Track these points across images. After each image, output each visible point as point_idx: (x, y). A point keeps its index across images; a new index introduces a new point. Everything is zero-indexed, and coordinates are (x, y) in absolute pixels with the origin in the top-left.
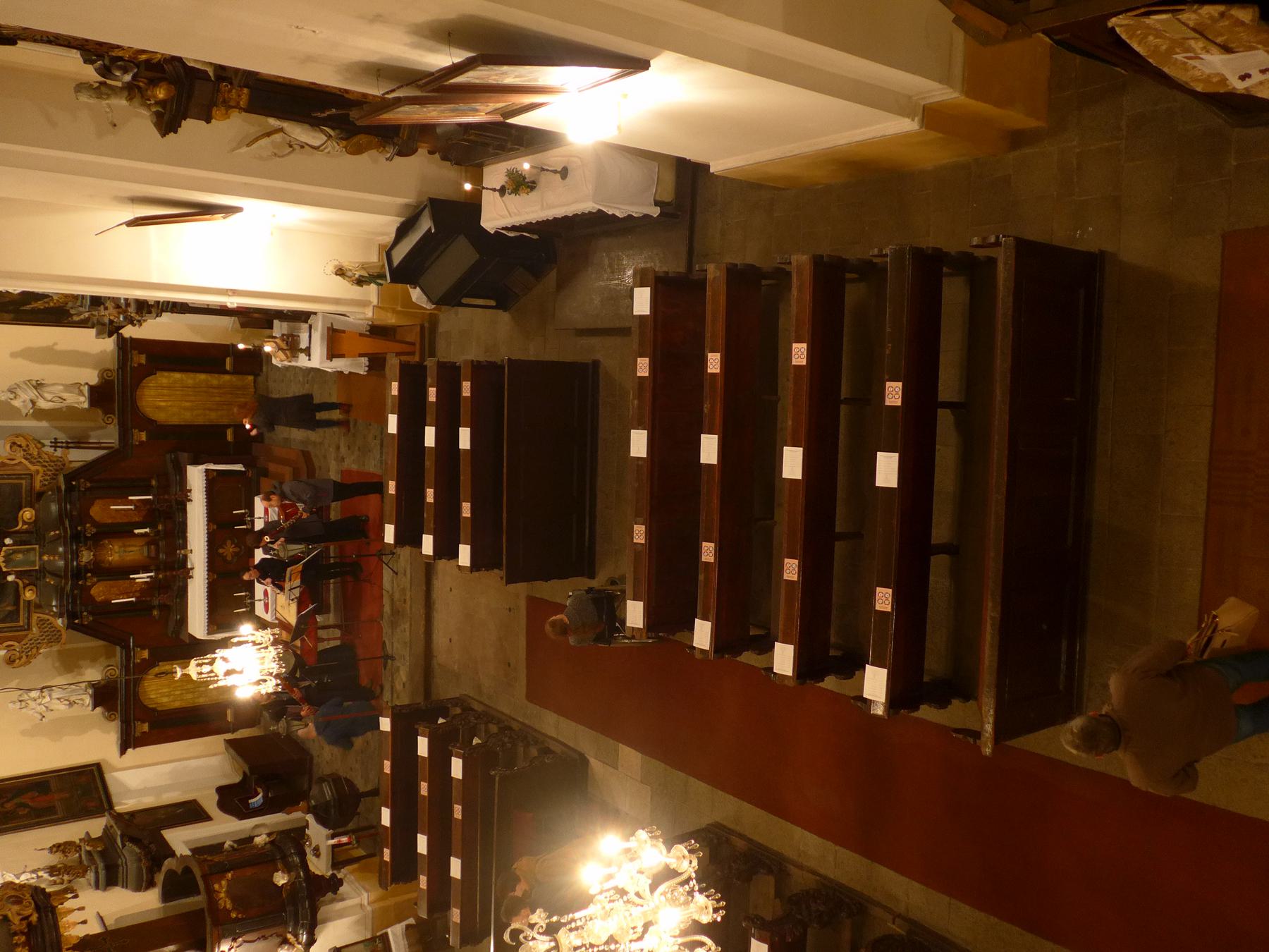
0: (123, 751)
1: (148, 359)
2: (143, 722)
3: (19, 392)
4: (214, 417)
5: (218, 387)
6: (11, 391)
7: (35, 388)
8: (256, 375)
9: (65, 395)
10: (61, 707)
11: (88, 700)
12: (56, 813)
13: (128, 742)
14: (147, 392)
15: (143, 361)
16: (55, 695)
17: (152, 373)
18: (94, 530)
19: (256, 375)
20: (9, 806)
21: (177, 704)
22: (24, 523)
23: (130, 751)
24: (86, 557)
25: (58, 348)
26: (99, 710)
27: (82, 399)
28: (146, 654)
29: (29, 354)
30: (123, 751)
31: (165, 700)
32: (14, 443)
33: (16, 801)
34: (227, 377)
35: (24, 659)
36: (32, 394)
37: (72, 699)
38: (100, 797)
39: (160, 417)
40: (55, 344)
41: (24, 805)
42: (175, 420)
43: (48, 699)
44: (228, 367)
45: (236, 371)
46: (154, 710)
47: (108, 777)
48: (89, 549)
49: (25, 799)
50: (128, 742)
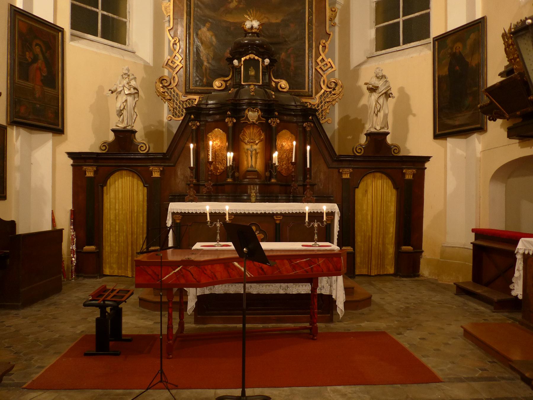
0: (71, 155)
1: (409, 180)
2: (95, 172)
3: (383, 80)
4: (358, 239)
5: (384, 244)
6: (383, 77)
7: (386, 93)
8: (395, 275)
9: (381, 114)
10: (119, 104)
11: (121, 126)
12: (20, 78)
13: (79, 159)
14: (379, 183)
15: (407, 177)
16: (130, 99)
17: (396, 186)
18: (274, 125)
19: (395, 275)
20: (37, 49)
21: (107, 205)
22: (277, 83)
23: (71, 162)
24: (253, 115)
25: (411, 118)
26: (111, 137)
27: (378, 128)
28: (156, 174)
29: (404, 97)
30: (71, 155)
31: (112, 194)
32: (336, 84)
33: (41, 56)
34: (391, 250)
35: (162, 90)
36: (382, 89)
37: (125, 112)
38: (29, 119)
39: (359, 193)
40: (414, 115)
41: (35, 59)
42: (357, 207)
43: (127, 92)
44: (405, 248)
45: (399, 254)
46: (105, 183)
47: (50, 135)
48: (259, 119)
49: (40, 63)
50: (79, 159)
